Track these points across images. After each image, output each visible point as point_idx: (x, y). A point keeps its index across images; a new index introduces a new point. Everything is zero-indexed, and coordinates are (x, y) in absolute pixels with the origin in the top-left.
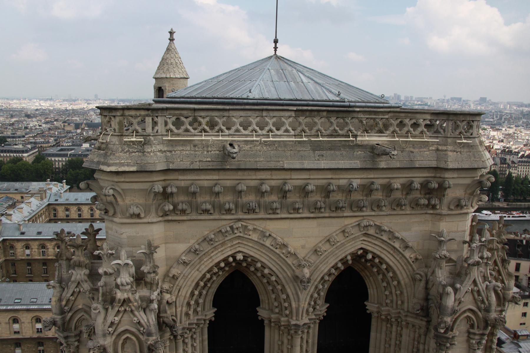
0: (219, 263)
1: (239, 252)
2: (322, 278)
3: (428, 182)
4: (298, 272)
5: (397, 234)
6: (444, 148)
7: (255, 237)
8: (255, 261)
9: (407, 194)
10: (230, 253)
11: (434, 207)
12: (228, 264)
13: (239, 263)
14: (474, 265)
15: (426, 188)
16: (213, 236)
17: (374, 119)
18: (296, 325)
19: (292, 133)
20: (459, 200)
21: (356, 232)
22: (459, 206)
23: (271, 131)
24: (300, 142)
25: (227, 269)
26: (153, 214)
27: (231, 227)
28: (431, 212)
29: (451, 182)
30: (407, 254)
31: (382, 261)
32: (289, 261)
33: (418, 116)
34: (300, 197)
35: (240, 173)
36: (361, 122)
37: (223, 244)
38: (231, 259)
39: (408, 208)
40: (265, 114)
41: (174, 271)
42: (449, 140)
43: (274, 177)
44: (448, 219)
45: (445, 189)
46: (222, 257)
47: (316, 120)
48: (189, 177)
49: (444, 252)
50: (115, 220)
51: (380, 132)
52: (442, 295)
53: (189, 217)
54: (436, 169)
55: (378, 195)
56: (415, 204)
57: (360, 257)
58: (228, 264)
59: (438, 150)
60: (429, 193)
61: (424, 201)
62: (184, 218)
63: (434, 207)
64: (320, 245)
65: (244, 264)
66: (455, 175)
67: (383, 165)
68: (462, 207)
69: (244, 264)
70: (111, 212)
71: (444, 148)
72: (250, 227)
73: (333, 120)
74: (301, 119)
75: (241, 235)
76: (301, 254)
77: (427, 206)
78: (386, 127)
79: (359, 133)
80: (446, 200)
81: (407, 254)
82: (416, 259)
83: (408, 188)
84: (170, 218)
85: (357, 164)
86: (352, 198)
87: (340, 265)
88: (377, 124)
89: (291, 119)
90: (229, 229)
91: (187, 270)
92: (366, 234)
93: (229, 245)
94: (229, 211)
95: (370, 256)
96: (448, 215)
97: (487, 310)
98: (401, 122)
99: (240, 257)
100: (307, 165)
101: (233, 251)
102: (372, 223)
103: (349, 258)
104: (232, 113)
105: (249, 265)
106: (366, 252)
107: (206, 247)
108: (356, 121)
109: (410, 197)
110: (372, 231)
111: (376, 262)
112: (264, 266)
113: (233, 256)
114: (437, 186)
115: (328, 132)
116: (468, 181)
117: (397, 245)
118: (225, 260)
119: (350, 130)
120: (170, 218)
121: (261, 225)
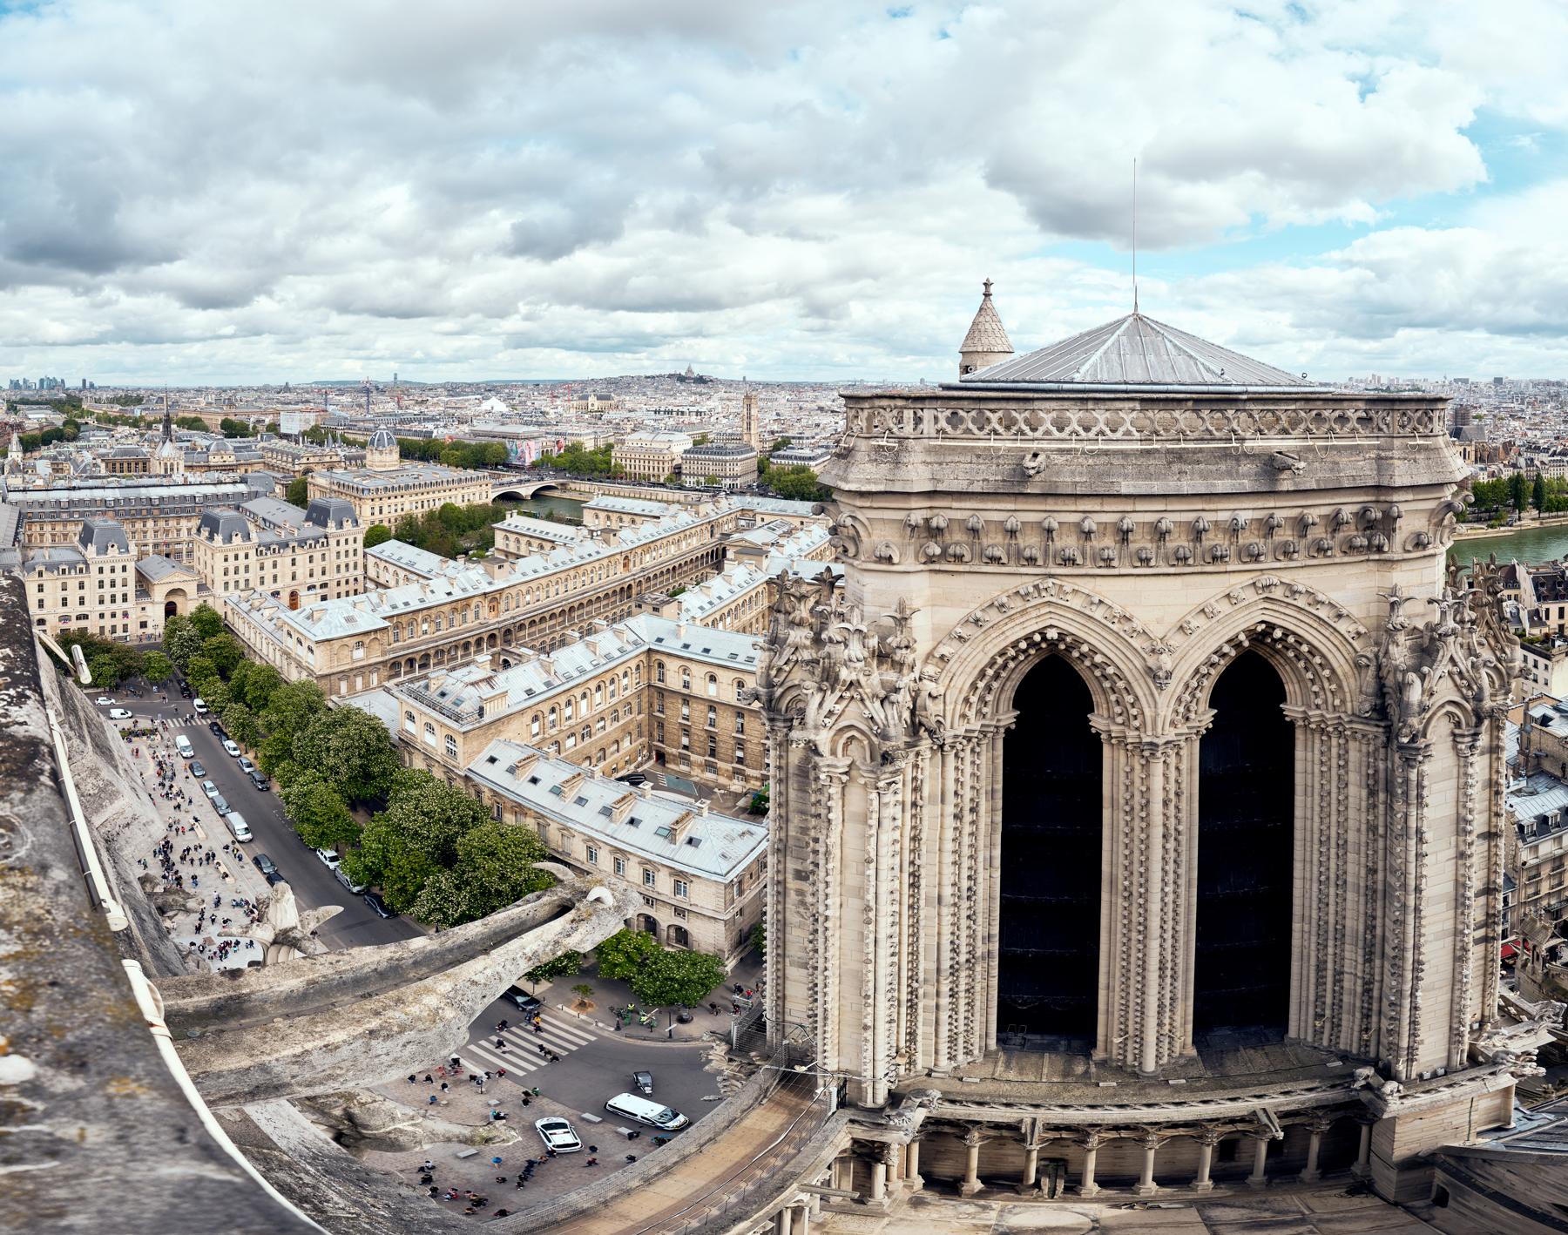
0: (1018, 641)
1: (1051, 626)
2: (1197, 671)
3: (1366, 510)
4: (1151, 662)
5: (1320, 597)
6: (1389, 454)
7: (1076, 602)
8: (1078, 642)
9: (1334, 530)
10: (1036, 628)
11: (1380, 549)
12: (1032, 644)
13: (1053, 644)
14: (1446, 635)
15: (1366, 523)
16: (1005, 600)
17: (1273, 411)
18: (1151, 744)
19: (1137, 436)
20: (1419, 535)
21: (1251, 596)
22: (1419, 544)
23: (1102, 433)
24: (1148, 452)
25: (1032, 652)
26: (911, 559)
27: (1036, 587)
28: (1376, 557)
29: (1403, 507)
30: (1342, 626)
31: (1300, 640)
32: (1136, 643)
33: (1345, 405)
34: (1151, 541)
35: (1050, 500)
36: (1251, 416)
37: (1024, 612)
38: (1037, 638)
39: (1338, 554)
40: (1090, 405)
41: (944, 650)
42: (1397, 442)
43: (1106, 508)
44: (1405, 566)
45: (1395, 519)
46: (1023, 634)
47: (1177, 414)
48: (968, 505)
49: (1401, 619)
50: (856, 563)
51: (1285, 431)
52: (1402, 687)
53: (967, 568)
54: (1378, 488)
55: (1285, 535)
56: (1350, 548)
57: (1262, 636)
58: (1032, 644)
59: (1379, 458)
60: (1370, 528)
61: (1361, 541)
62: (961, 568)
63: (1380, 549)
64: (1188, 618)
65: (1062, 647)
66: (1410, 497)
67: (1286, 485)
68: (1425, 547)
69: (1062, 647)
70: (852, 551)
71: (1389, 454)
72: (1068, 588)
73: (1205, 413)
74: (1150, 414)
75: (1053, 599)
76: (1157, 631)
77: (1369, 547)
78: (1294, 423)
79: (1248, 435)
80: (1399, 537)
81: (1342, 626)
82: (1359, 634)
83: (1335, 522)
84: (937, 567)
85: (1247, 485)
86: (1241, 541)
87: (1226, 649)
88: (1278, 419)
89: (1134, 414)
90: (1031, 589)
91: (965, 649)
92: (1267, 599)
93: (1034, 614)
94: (1031, 560)
95: (1278, 634)
96: (1404, 560)
97: (1478, 698)
98: (1318, 415)
99: (1052, 634)
100: (1156, 487)
101: (1041, 625)
102: (1276, 581)
103: (1242, 637)
104: (1037, 405)
105: (1069, 649)
106: (1271, 627)
107: (994, 616)
108: (1243, 416)
109: (1340, 536)
110: (1278, 593)
111: (1290, 643)
112: (1094, 650)
113: (1042, 633)
114: (1379, 515)
115: (1196, 435)
116: (1432, 505)
117: (1323, 613)
118: (1028, 638)
119: (1234, 431)
120: (937, 567)
121: (1086, 585)
